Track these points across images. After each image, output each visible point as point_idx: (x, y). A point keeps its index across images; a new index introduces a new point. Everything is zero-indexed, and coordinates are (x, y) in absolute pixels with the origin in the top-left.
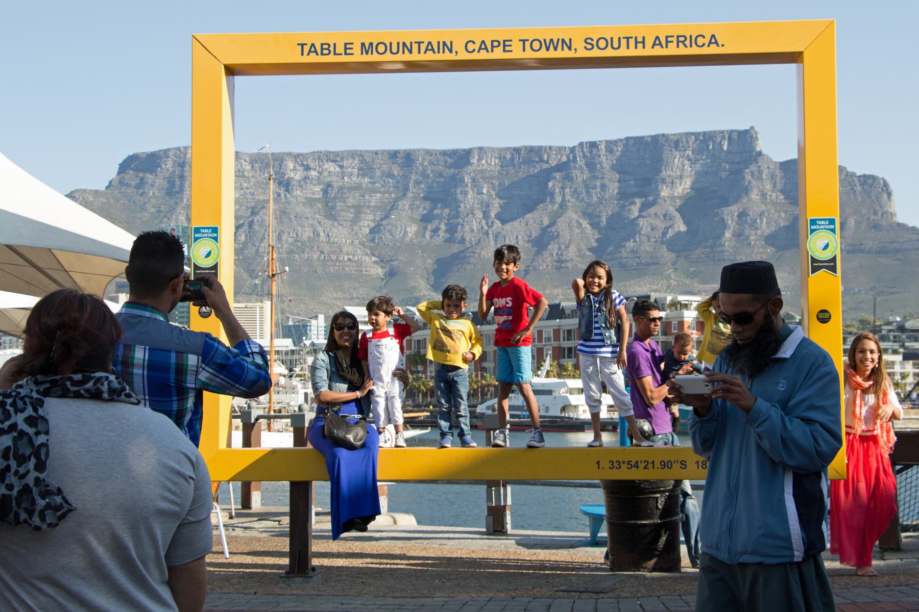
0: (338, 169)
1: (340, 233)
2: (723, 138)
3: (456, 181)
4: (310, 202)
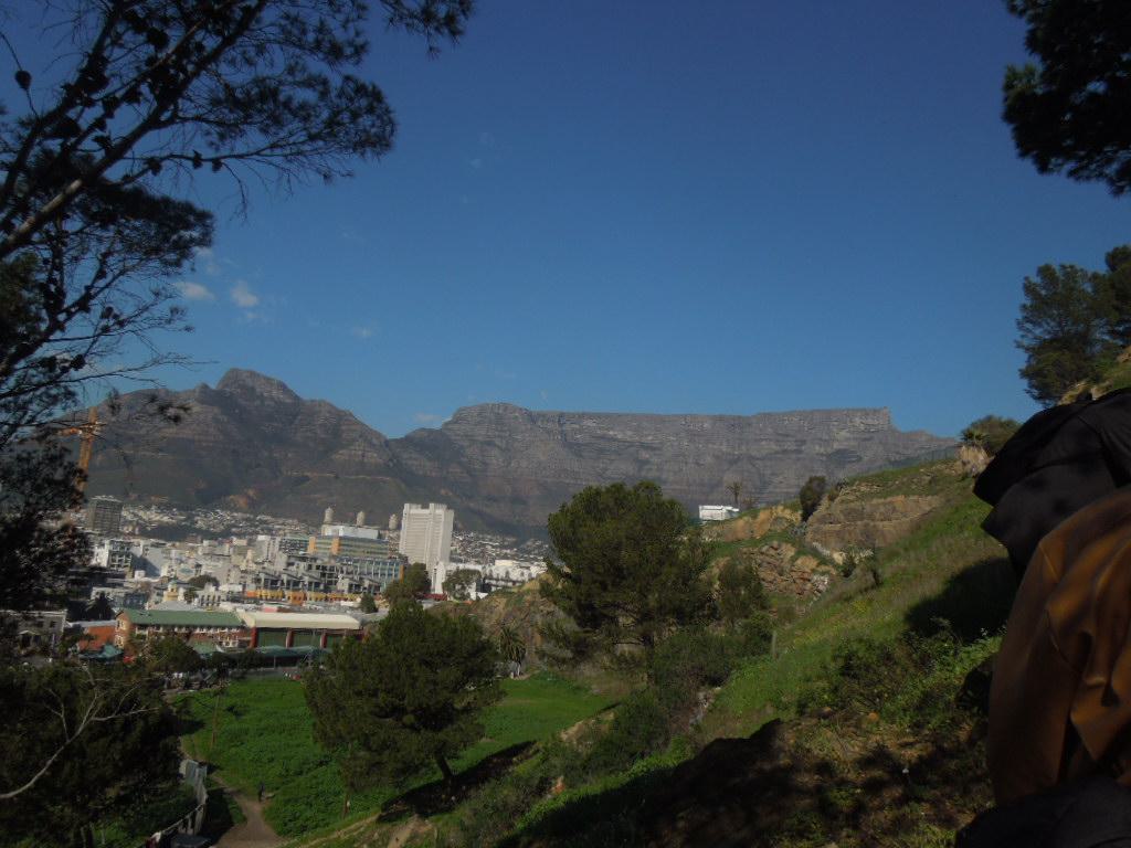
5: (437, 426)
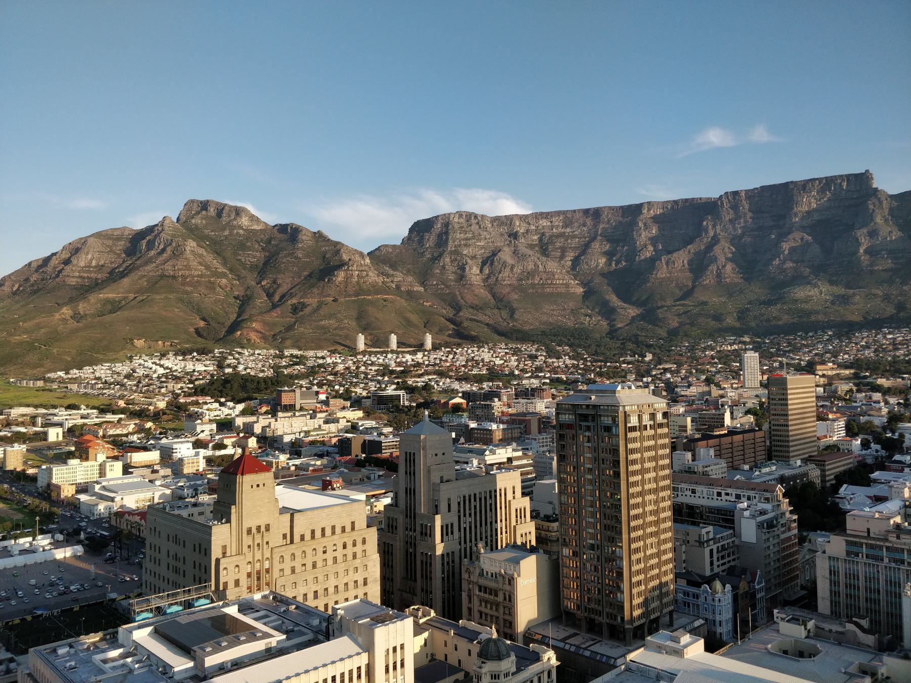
0: (549, 224)
1: (552, 266)
2: (843, 180)
3: (633, 224)
4: (531, 246)
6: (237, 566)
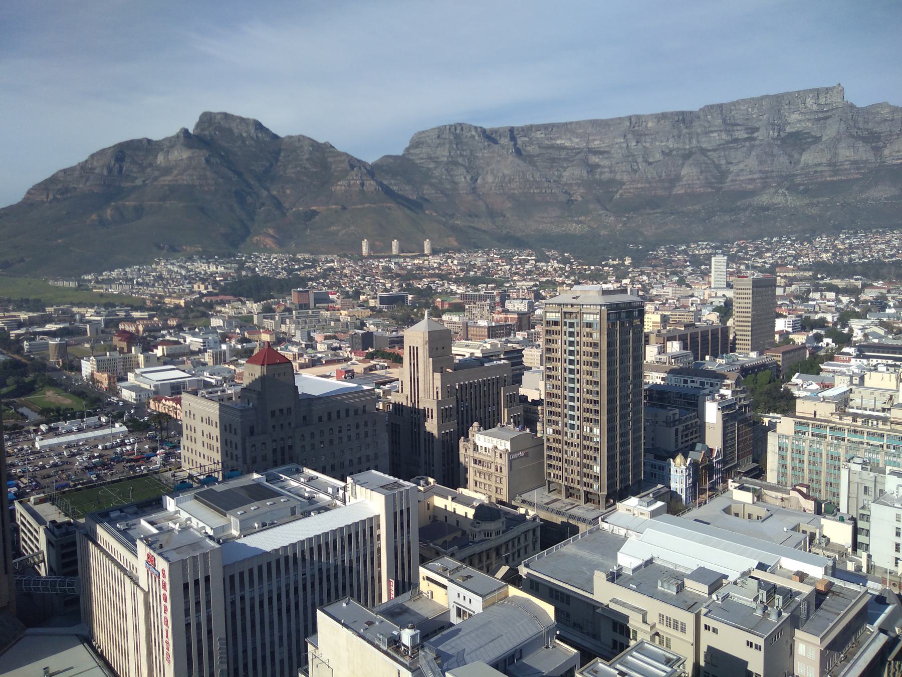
5: (400, 152)
6: (264, 443)
